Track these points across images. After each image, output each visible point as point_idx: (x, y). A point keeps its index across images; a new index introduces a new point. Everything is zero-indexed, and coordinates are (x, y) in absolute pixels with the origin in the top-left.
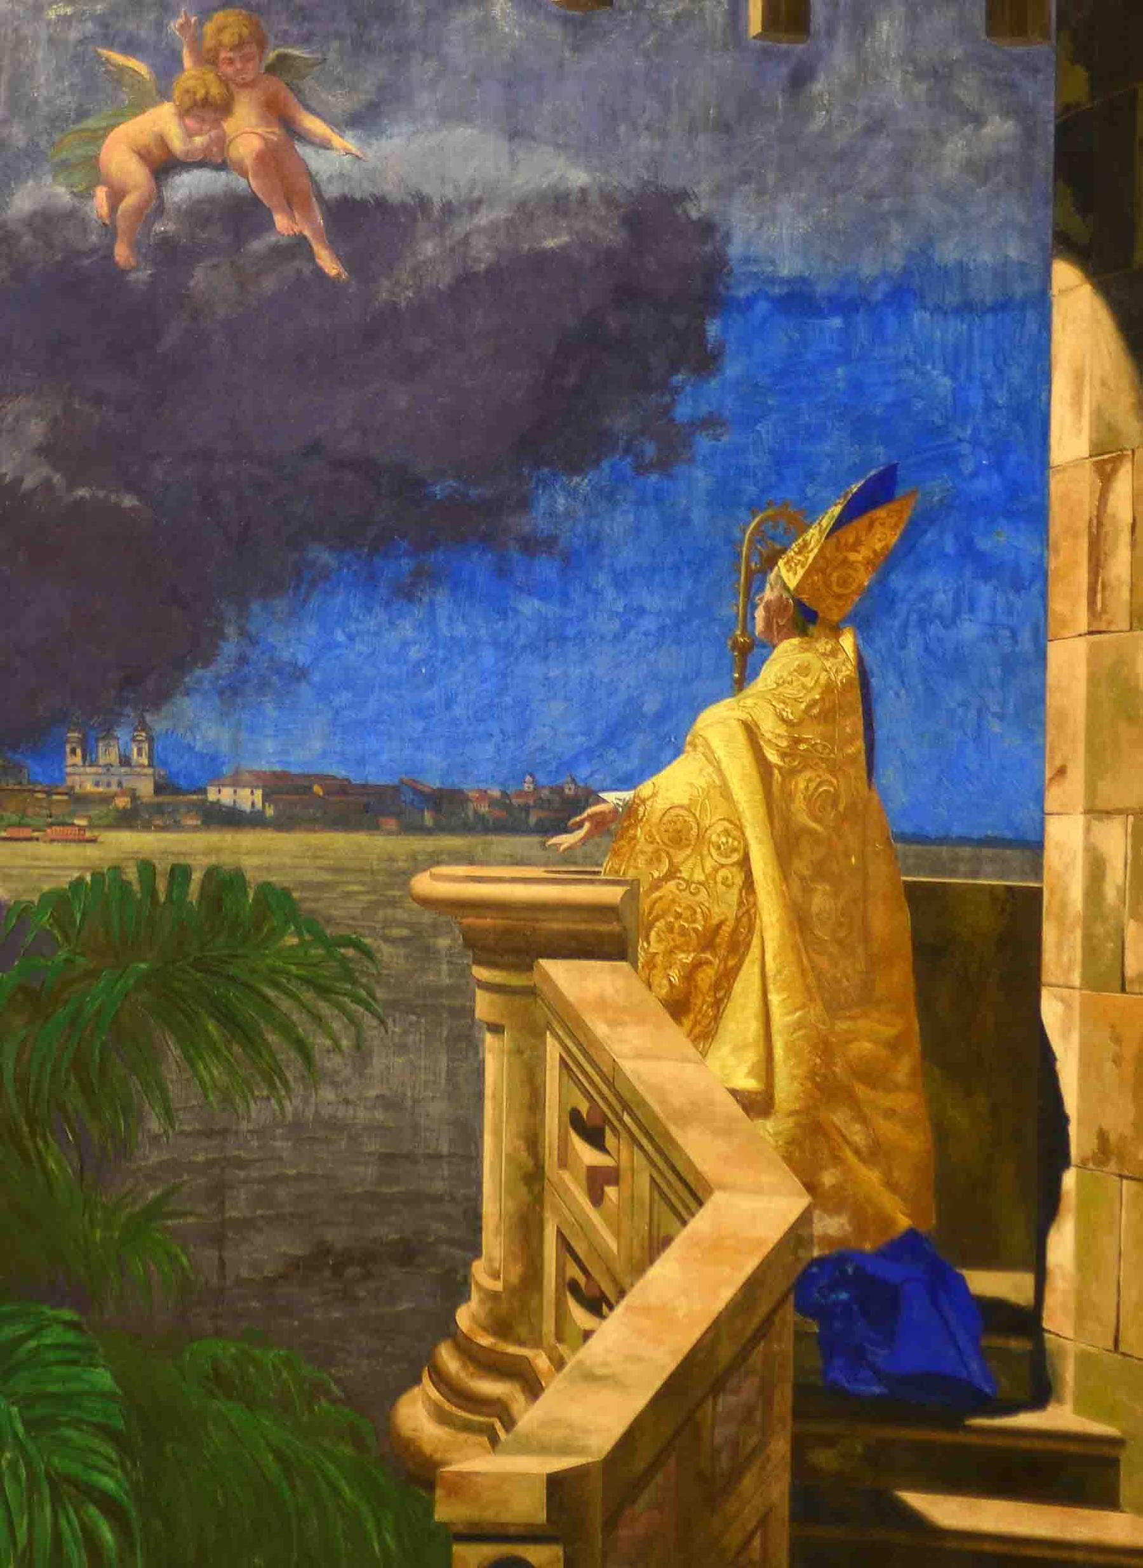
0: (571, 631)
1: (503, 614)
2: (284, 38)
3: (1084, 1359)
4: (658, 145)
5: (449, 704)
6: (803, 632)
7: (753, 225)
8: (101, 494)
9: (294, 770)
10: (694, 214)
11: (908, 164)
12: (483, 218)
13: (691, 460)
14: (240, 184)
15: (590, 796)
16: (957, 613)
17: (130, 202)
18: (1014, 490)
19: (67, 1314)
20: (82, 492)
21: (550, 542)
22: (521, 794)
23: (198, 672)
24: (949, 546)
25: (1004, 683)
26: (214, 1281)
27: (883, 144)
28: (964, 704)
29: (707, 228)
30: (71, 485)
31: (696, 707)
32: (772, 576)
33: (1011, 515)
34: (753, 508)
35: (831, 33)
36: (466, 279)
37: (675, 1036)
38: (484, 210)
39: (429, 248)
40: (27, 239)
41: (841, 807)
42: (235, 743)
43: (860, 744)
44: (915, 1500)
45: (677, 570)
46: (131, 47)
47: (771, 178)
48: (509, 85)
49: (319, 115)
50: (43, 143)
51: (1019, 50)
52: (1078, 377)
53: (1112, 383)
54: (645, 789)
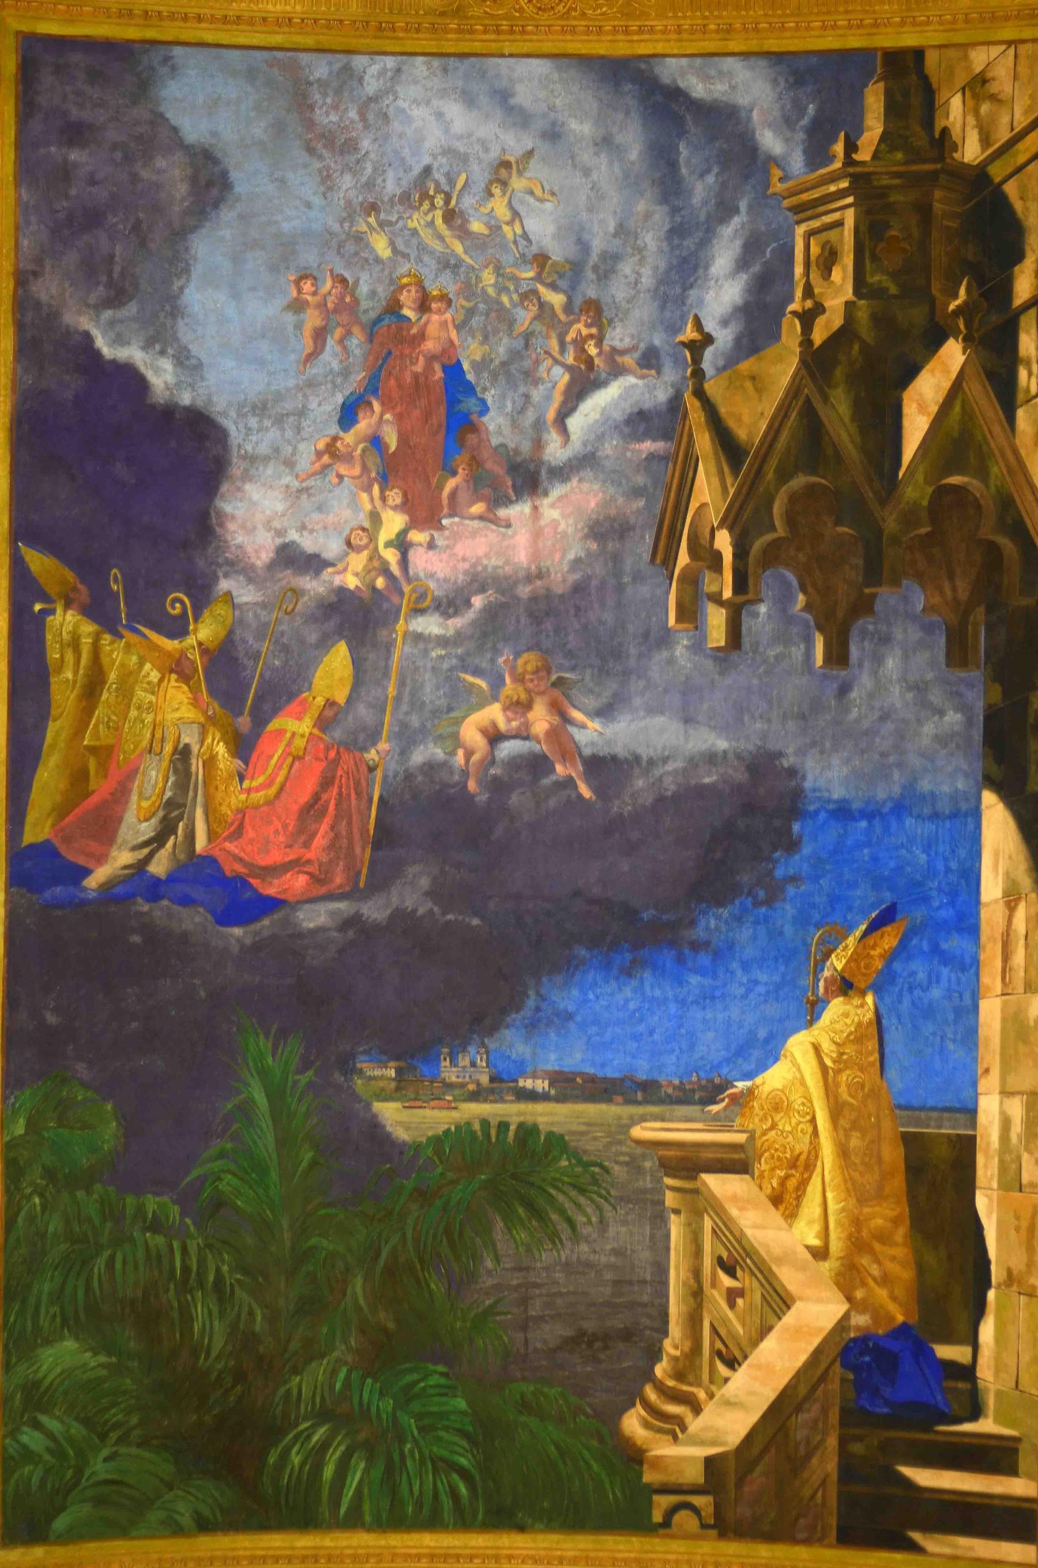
0: (718, 993)
1: (680, 983)
2: (561, 668)
3: (999, 1394)
4: (766, 727)
5: (651, 1033)
6: (845, 994)
7: (818, 771)
8: (461, 918)
9: (566, 1069)
10: (786, 765)
11: (902, 738)
12: (670, 767)
13: (784, 900)
14: (536, 748)
15: (728, 1084)
16: (930, 983)
17: (476, 757)
18: (961, 917)
19: (441, 1368)
20: (450, 917)
21: (708, 943)
22: (691, 1083)
23: (514, 1016)
24: (925, 946)
25: (955, 1022)
26: (522, 1351)
27: (889, 726)
28: (934, 1034)
29: (792, 772)
30: (444, 914)
31: (786, 1037)
32: (828, 963)
33: (960, 930)
34: (818, 926)
35: (860, 666)
36: (660, 800)
37: (775, 1216)
38: (670, 763)
39: (640, 783)
40: (420, 778)
41: (866, 1090)
42: (534, 1054)
43: (876, 1055)
44: (907, 1471)
45: (776, 959)
46: (477, 672)
47: (828, 745)
48: (684, 693)
49: (579, 710)
50: (429, 725)
51: (963, 675)
52: (996, 854)
53: (1014, 857)
54: (758, 1080)
